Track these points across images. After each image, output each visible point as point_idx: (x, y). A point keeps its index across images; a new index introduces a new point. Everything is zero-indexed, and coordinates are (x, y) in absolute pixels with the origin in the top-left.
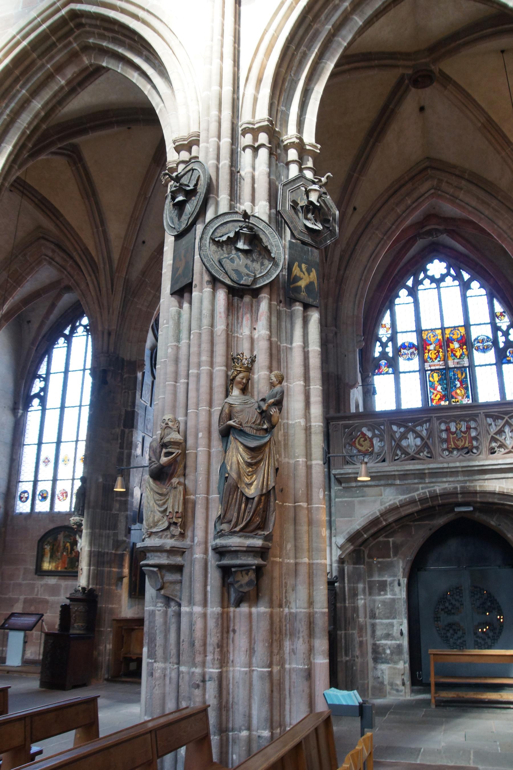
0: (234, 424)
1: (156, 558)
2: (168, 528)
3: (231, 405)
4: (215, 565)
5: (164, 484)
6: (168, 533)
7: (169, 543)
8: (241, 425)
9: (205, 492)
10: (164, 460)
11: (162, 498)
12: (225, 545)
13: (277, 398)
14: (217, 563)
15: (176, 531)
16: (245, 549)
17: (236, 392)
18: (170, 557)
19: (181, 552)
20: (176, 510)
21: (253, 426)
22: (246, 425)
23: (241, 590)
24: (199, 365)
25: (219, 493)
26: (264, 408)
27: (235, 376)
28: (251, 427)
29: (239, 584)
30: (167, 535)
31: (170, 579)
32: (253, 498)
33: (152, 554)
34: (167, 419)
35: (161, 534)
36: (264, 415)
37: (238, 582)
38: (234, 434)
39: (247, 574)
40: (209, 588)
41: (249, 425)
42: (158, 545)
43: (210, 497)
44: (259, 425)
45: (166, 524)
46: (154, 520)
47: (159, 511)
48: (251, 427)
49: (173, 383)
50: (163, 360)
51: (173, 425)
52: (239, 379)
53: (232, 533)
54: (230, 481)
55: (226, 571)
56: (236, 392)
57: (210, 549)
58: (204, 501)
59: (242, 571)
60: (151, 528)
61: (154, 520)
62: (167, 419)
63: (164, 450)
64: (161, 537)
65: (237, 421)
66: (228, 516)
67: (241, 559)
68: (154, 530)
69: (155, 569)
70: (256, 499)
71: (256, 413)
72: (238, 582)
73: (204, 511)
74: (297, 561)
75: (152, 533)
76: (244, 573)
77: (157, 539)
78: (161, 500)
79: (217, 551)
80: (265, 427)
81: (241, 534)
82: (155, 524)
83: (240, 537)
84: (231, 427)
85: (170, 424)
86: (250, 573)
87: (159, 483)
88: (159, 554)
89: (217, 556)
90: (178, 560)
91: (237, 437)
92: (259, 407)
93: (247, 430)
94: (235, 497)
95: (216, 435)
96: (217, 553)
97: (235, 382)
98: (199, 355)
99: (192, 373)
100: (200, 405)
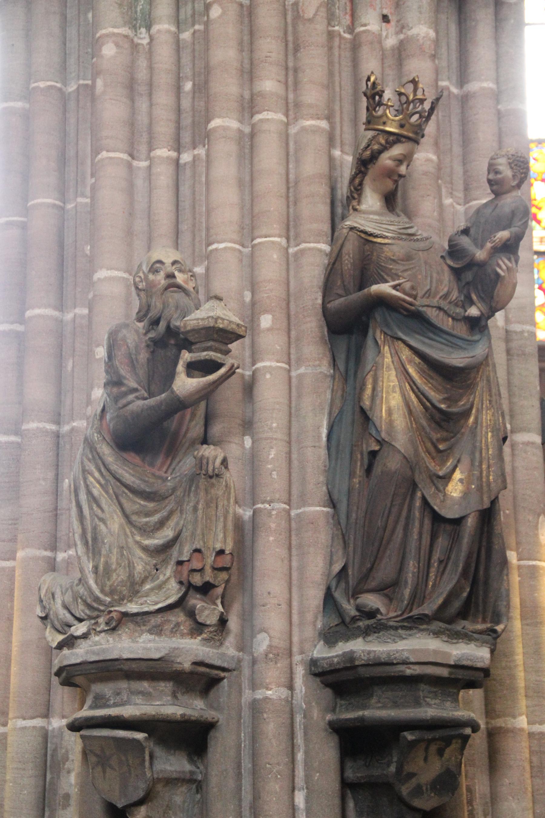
0: (394, 292)
1: (138, 699)
2: (179, 604)
3: (366, 239)
4: (323, 724)
5: (152, 465)
6: (179, 617)
7: (189, 649)
8: (415, 297)
9: (285, 497)
10: (185, 384)
11: (151, 505)
12: (384, 658)
13: (513, 229)
14: (329, 717)
15: (209, 613)
16: (444, 672)
17: (371, 200)
18: (179, 695)
19: (204, 680)
20: (218, 546)
21: (444, 304)
22: (426, 301)
23: (417, 803)
24: (249, 106)
25: (332, 503)
26: (480, 255)
27: (380, 152)
28: (440, 308)
29: (414, 782)
30: (178, 625)
31: (169, 768)
32: (458, 522)
33: (123, 685)
34: (168, 261)
35: (158, 619)
36: (469, 276)
37: (411, 775)
38: (388, 325)
39: (440, 753)
40: (300, 799)
41: (435, 301)
42: (157, 656)
43: (293, 513)
44: (456, 305)
45: (173, 592)
46: (131, 576)
47: (145, 549)
48: (440, 308)
49: (125, 156)
50: (42, 85)
51: (186, 282)
52: (389, 163)
53: (414, 623)
54: (392, 463)
55: (356, 742)
56: (371, 200)
57: (300, 672)
58: (284, 524)
59: (429, 742)
60: (121, 600)
61: (131, 576)
62: (168, 261)
63: (186, 356)
64: (158, 630)
65: (407, 286)
66: (385, 571)
67: (429, 705)
68: (133, 608)
69: (140, 736)
70: (471, 522)
71: (446, 268)
72: (411, 775)
73: (284, 553)
74: (499, 722)
75: (125, 615)
76: (433, 748)
77: (146, 636)
78: (148, 514)
79: (330, 678)
80: (473, 311)
81: (437, 625)
82: (134, 589)
83: (437, 634)
84: (382, 302)
85: (180, 278)
86: (448, 752)
87: (137, 460)
88: (145, 685)
89: (328, 693)
90: (193, 707)
91: (401, 335)
92: (454, 251)
93: (432, 314)
94: (404, 513)
95: (312, 325)
96: (327, 685)
97: (373, 171)
98: (249, 73)
99: (225, 129)
100: (256, 233)
